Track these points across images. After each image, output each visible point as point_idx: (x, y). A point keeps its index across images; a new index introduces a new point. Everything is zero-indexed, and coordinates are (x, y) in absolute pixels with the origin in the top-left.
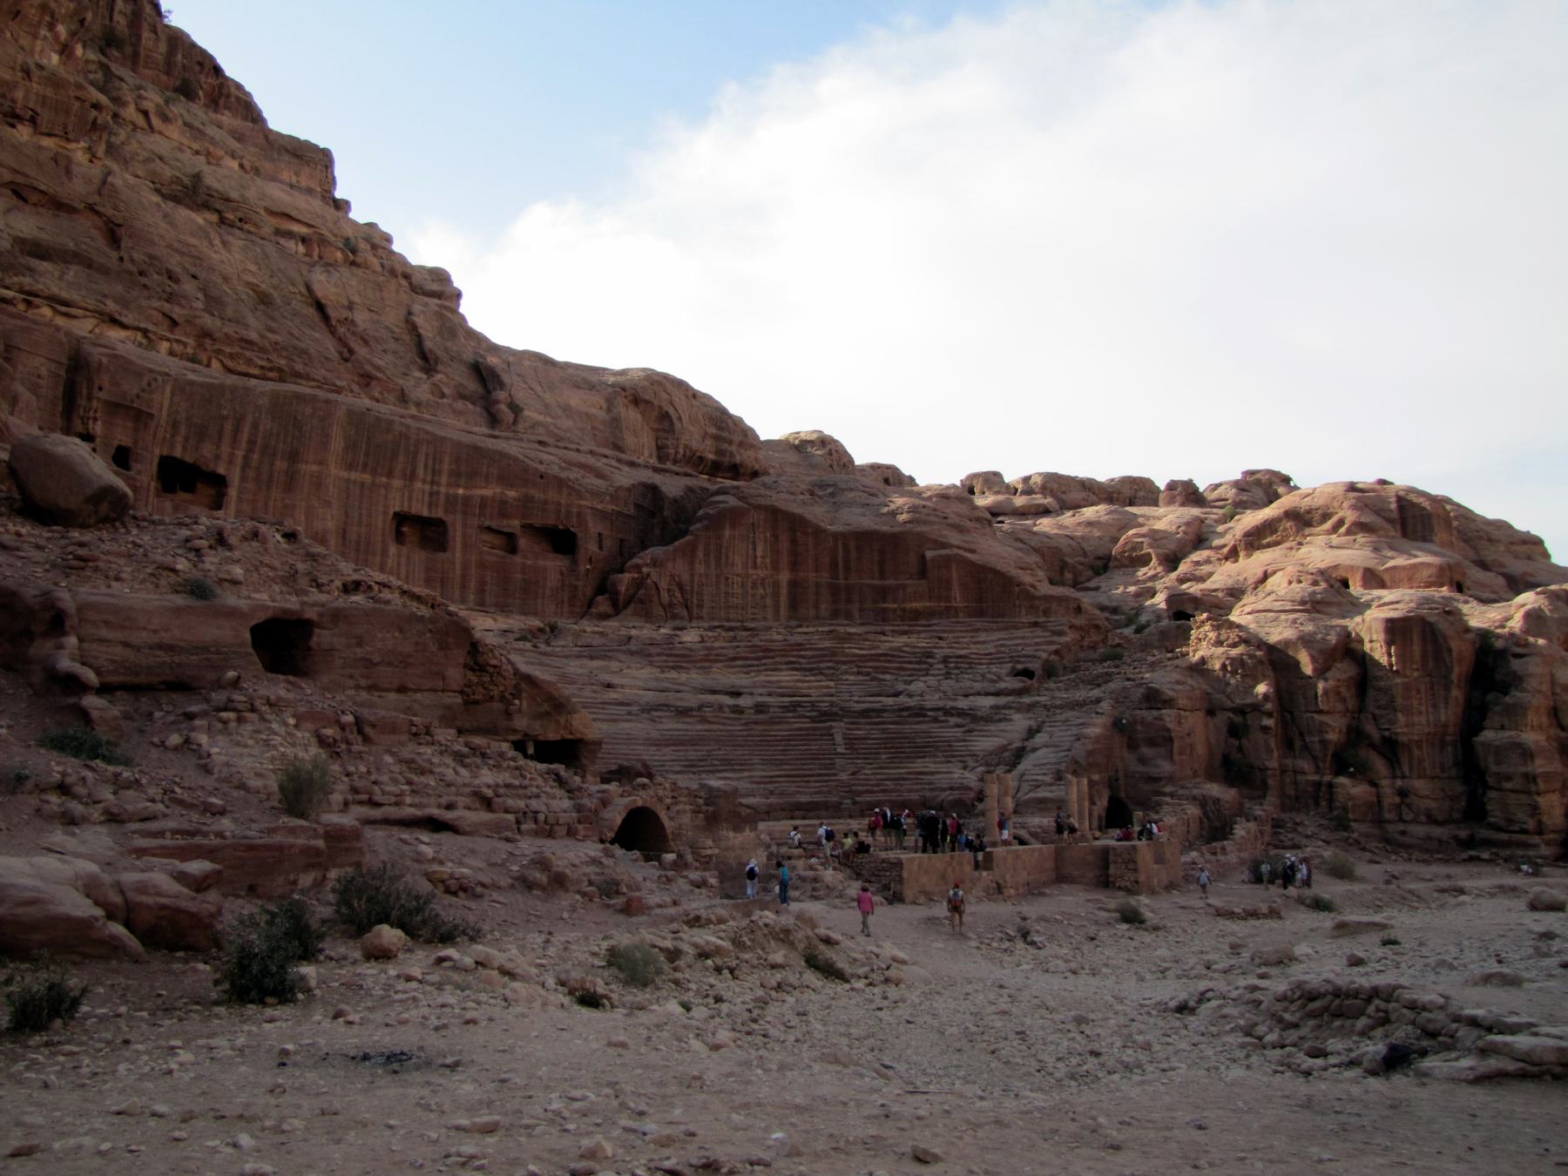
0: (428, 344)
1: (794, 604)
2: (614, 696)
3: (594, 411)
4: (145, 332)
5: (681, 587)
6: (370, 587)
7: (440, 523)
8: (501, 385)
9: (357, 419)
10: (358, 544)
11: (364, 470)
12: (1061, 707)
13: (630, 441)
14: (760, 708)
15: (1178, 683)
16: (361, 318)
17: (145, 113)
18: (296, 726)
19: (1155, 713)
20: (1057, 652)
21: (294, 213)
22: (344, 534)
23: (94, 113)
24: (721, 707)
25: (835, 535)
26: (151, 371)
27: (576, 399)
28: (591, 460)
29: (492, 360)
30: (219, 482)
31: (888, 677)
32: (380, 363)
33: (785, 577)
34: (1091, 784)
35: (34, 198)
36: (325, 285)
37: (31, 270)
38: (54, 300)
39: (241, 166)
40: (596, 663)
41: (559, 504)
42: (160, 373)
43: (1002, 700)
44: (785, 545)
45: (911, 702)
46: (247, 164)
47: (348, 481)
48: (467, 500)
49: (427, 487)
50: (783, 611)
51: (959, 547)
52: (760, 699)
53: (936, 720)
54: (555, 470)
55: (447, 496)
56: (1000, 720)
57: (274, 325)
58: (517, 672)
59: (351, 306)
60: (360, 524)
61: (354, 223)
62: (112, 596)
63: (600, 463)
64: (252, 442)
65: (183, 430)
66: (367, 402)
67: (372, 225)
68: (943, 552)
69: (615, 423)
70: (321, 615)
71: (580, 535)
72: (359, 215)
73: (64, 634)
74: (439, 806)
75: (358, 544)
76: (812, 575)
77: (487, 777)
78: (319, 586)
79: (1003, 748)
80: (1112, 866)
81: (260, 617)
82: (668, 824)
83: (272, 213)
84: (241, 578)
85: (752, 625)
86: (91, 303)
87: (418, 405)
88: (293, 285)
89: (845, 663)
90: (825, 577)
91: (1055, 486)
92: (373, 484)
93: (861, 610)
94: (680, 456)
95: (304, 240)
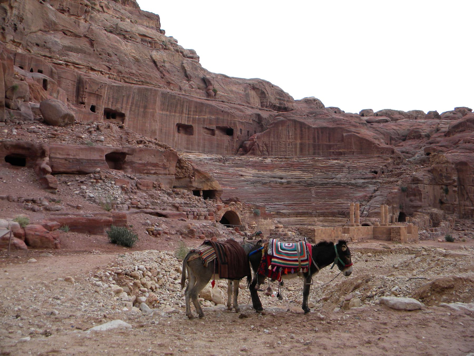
0: (188, 72)
1: (301, 150)
2: (243, 179)
3: (241, 92)
4: (101, 72)
5: (266, 145)
6: (145, 143)
7: (191, 127)
8: (211, 84)
9: (164, 95)
10: (166, 133)
11: (167, 111)
12: (385, 183)
13: (252, 100)
14: (288, 183)
15: (424, 175)
16: (167, 65)
17: (102, 7)
18: (115, 184)
19: (416, 185)
20: (385, 166)
21: (147, 35)
23: (86, 8)
24: (276, 183)
25: (314, 128)
26: (101, 83)
27: (234, 89)
28: (239, 107)
29: (208, 77)
30: (122, 116)
31: (330, 173)
32: (173, 78)
33: (298, 142)
34: (393, 208)
35: (69, 34)
36: (156, 55)
37: (68, 55)
38: (74, 63)
39: (131, 21)
40: (238, 169)
41: (228, 120)
42: (104, 83)
43: (366, 181)
44: (298, 131)
45: (337, 181)
46: (133, 20)
47: (162, 114)
48: (199, 119)
49: (187, 116)
50: (298, 153)
51: (354, 132)
52: (289, 180)
53: (344, 187)
54: (226, 110)
55: (193, 118)
56: (365, 187)
57: (140, 68)
58: (194, 169)
59: (164, 62)
60: (166, 127)
61: (166, 37)
62: (62, 145)
63: (241, 107)
64: (132, 103)
65: (111, 100)
66: (168, 90)
67: (171, 37)
68: (349, 134)
69: (247, 95)
70: (128, 151)
71: (234, 130)
72: (167, 34)
73: (45, 157)
74: (160, 209)
75: (166, 133)
76: (307, 141)
77: (178, 200)
78: (129, 142)
79: (366, 196)
80: (392, 234)
81: (109, 152)
82: (240, 217)
83: (140, 35)
84: (103, 140)
85: (288, 157)
86: (85, 64)
87: (185, 91)
89: (316, 169)
90: (311, 142)
91: (390, 113)
92: (170, 115)
93: (322, 152)
94: (268, 105)
95: (150, 43)
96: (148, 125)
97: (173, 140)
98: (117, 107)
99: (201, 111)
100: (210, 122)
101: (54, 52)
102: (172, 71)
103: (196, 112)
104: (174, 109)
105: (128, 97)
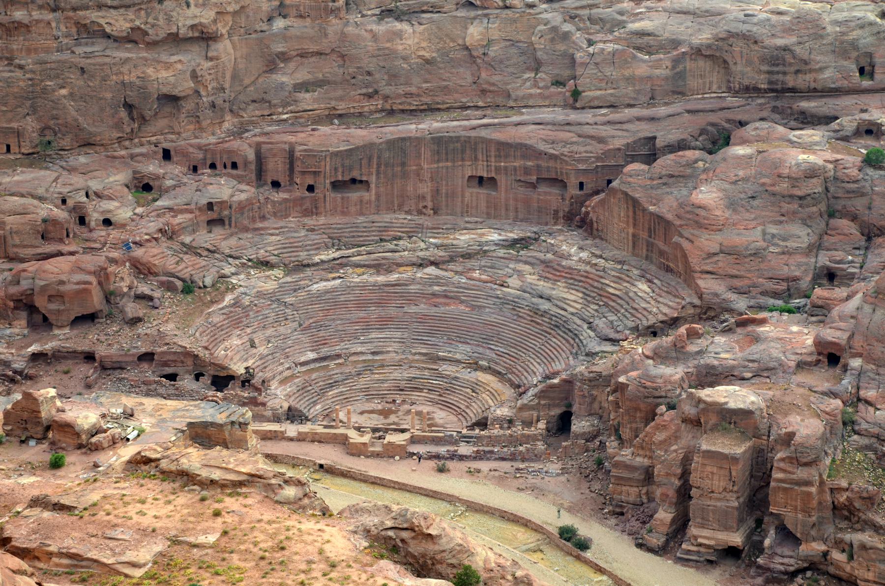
7: (492, 179)
11: (447, 160)
16: (494, 51)
22: (436, 192)
25: (652, 214)
33: (631, 230)
41: (556, 168)
44: (631, 214)
47: (438, 167)
48: (506, 168)
55: (496, 167)
59: (490, 42)
64: (379, 165)
69: (681, 76)
76: (641, 232)
88: (454, 41)
96: (410, 188)
97: (462, 202)
98: (356, 174)
99: (506, 156)
100: (527, 171)
101: (275, 106)
102: (501, 62)
103: (500, 156)
104: (460, 156)
105: (370, 159)
